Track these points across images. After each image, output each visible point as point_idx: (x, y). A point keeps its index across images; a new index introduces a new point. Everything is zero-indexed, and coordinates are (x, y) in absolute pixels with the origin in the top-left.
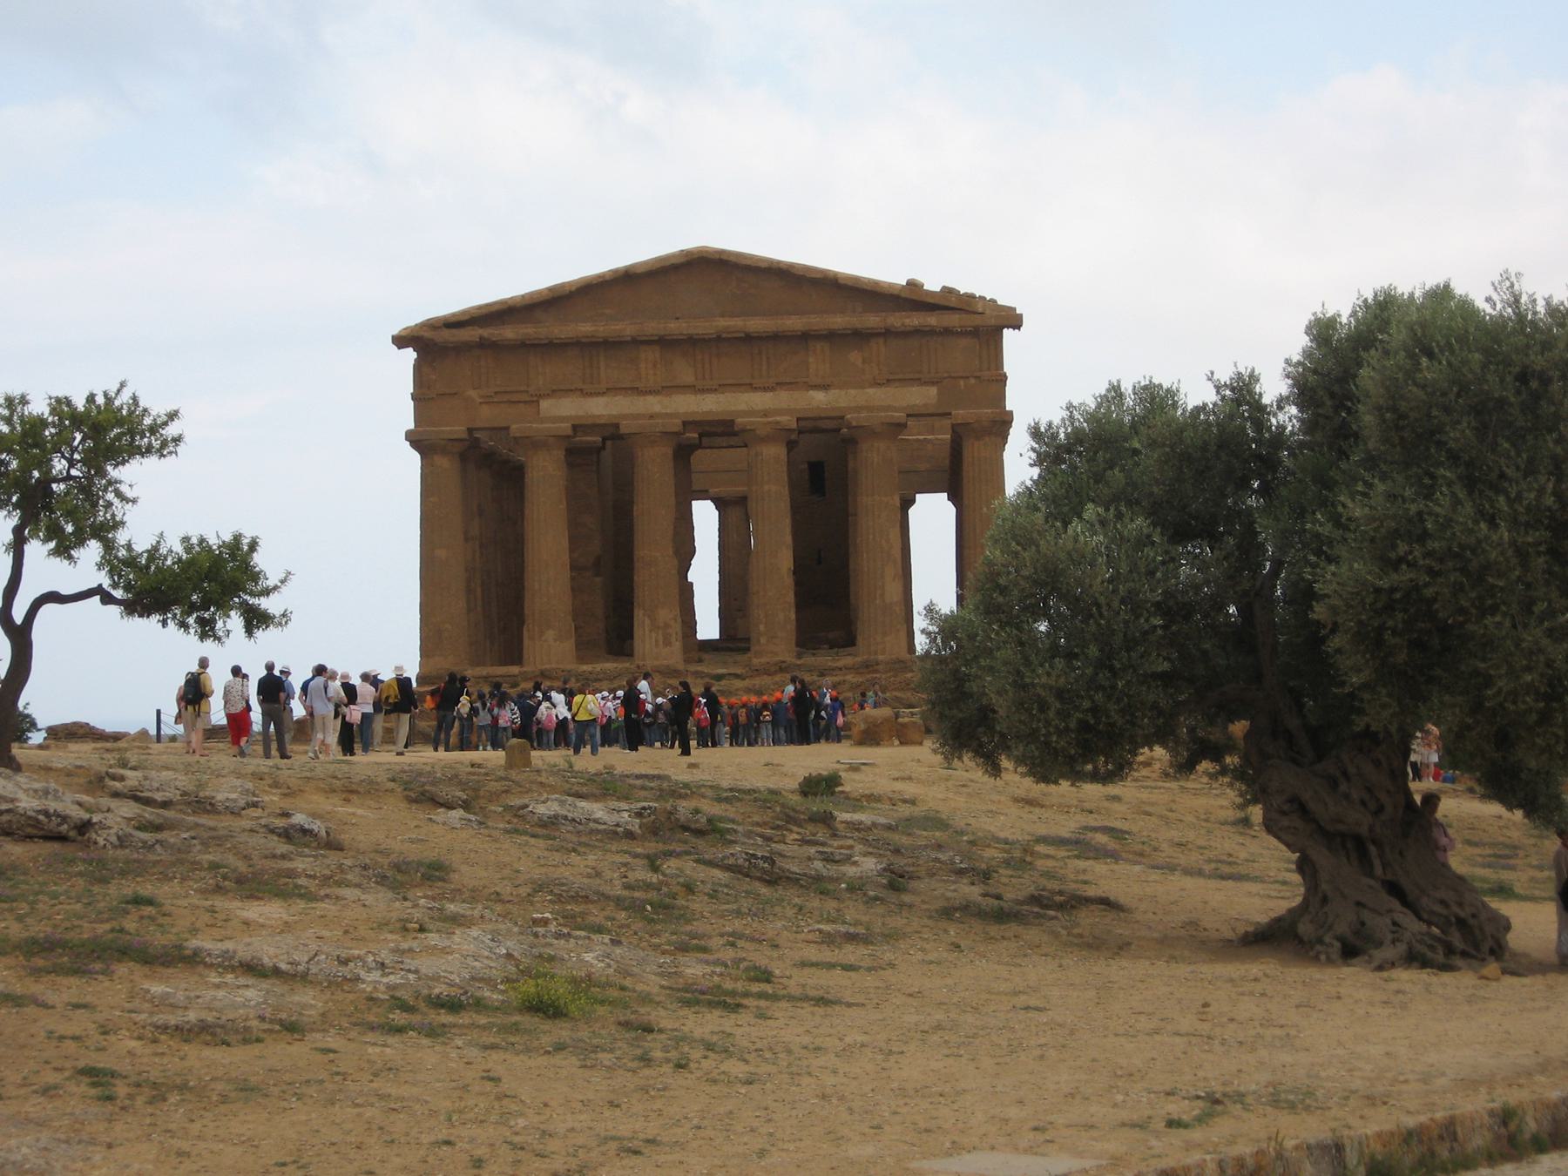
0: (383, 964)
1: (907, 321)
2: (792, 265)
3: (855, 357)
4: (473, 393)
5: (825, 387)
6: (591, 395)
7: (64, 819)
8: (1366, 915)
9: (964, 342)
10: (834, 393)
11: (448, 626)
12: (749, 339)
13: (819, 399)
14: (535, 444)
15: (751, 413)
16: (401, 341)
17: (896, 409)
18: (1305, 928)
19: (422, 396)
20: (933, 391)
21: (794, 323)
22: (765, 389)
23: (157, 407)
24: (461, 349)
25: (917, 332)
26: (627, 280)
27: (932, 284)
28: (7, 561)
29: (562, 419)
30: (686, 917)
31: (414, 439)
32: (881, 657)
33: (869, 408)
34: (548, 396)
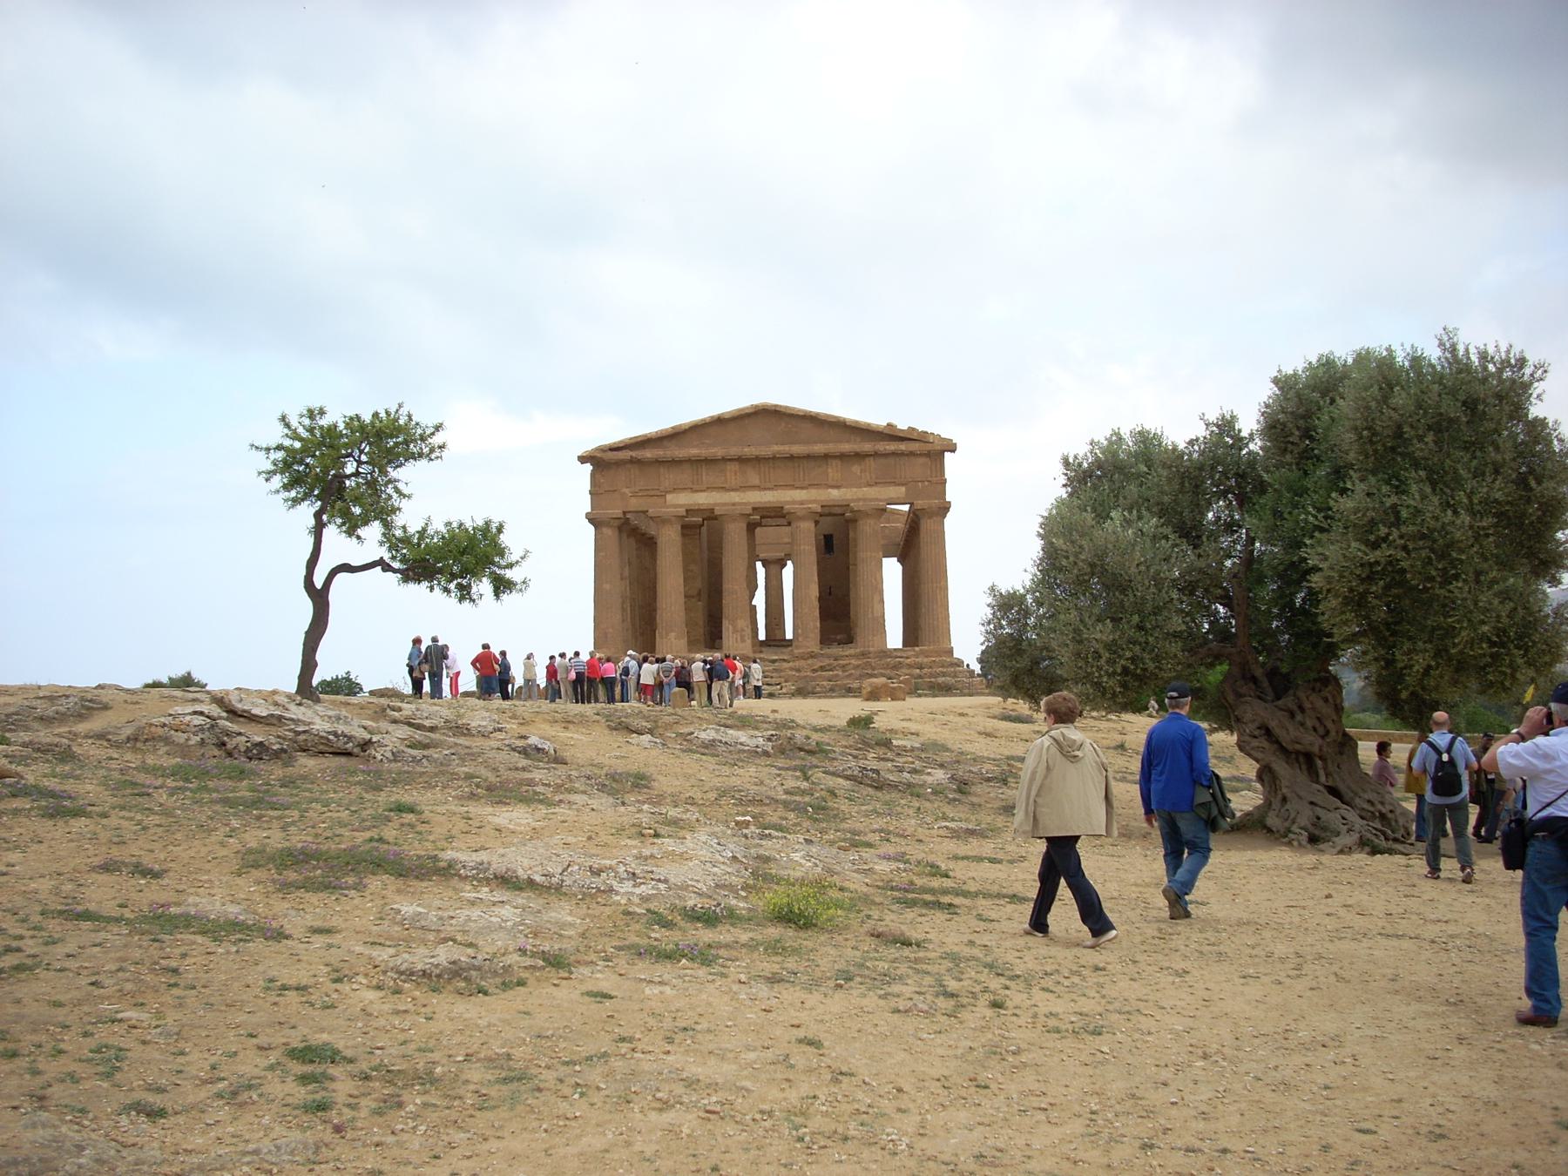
0: (634, 874)
1: (887, 447)
2: (818, 414)
3: (856, 469)
4: (627, 491)
5: (838, 487)
6: (697, 491)
7: (350, 738)
8: (1320, 812)
9: (922, 460)
10: (843, 490)
11: (611, 630)
12: (792, 458)
13: (835, 494)
14: (661, 521)
15: (794, 502)
16: (583, 459)
17: (881, 500)
18: (1272, 821)
19: (594, 493)
20: (903, 489)
21: (819, 448)
22: (802, 488)
23: (424, 418)
24: (619, 464)
25: (894, 454)
26: (719, 421)
27: (902, 425)
28: (311, 540)
29: (681, 506)
30: (839, 817)
31: (591, 519)
32: (871, 649)
33: (865, 500)
34: (670, 492)
